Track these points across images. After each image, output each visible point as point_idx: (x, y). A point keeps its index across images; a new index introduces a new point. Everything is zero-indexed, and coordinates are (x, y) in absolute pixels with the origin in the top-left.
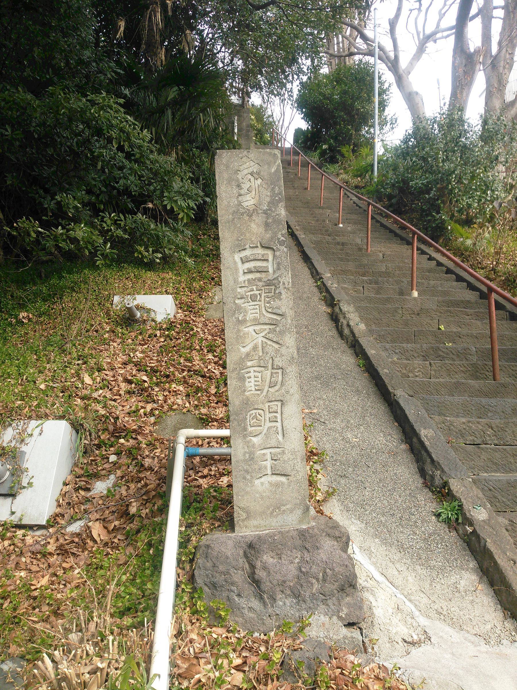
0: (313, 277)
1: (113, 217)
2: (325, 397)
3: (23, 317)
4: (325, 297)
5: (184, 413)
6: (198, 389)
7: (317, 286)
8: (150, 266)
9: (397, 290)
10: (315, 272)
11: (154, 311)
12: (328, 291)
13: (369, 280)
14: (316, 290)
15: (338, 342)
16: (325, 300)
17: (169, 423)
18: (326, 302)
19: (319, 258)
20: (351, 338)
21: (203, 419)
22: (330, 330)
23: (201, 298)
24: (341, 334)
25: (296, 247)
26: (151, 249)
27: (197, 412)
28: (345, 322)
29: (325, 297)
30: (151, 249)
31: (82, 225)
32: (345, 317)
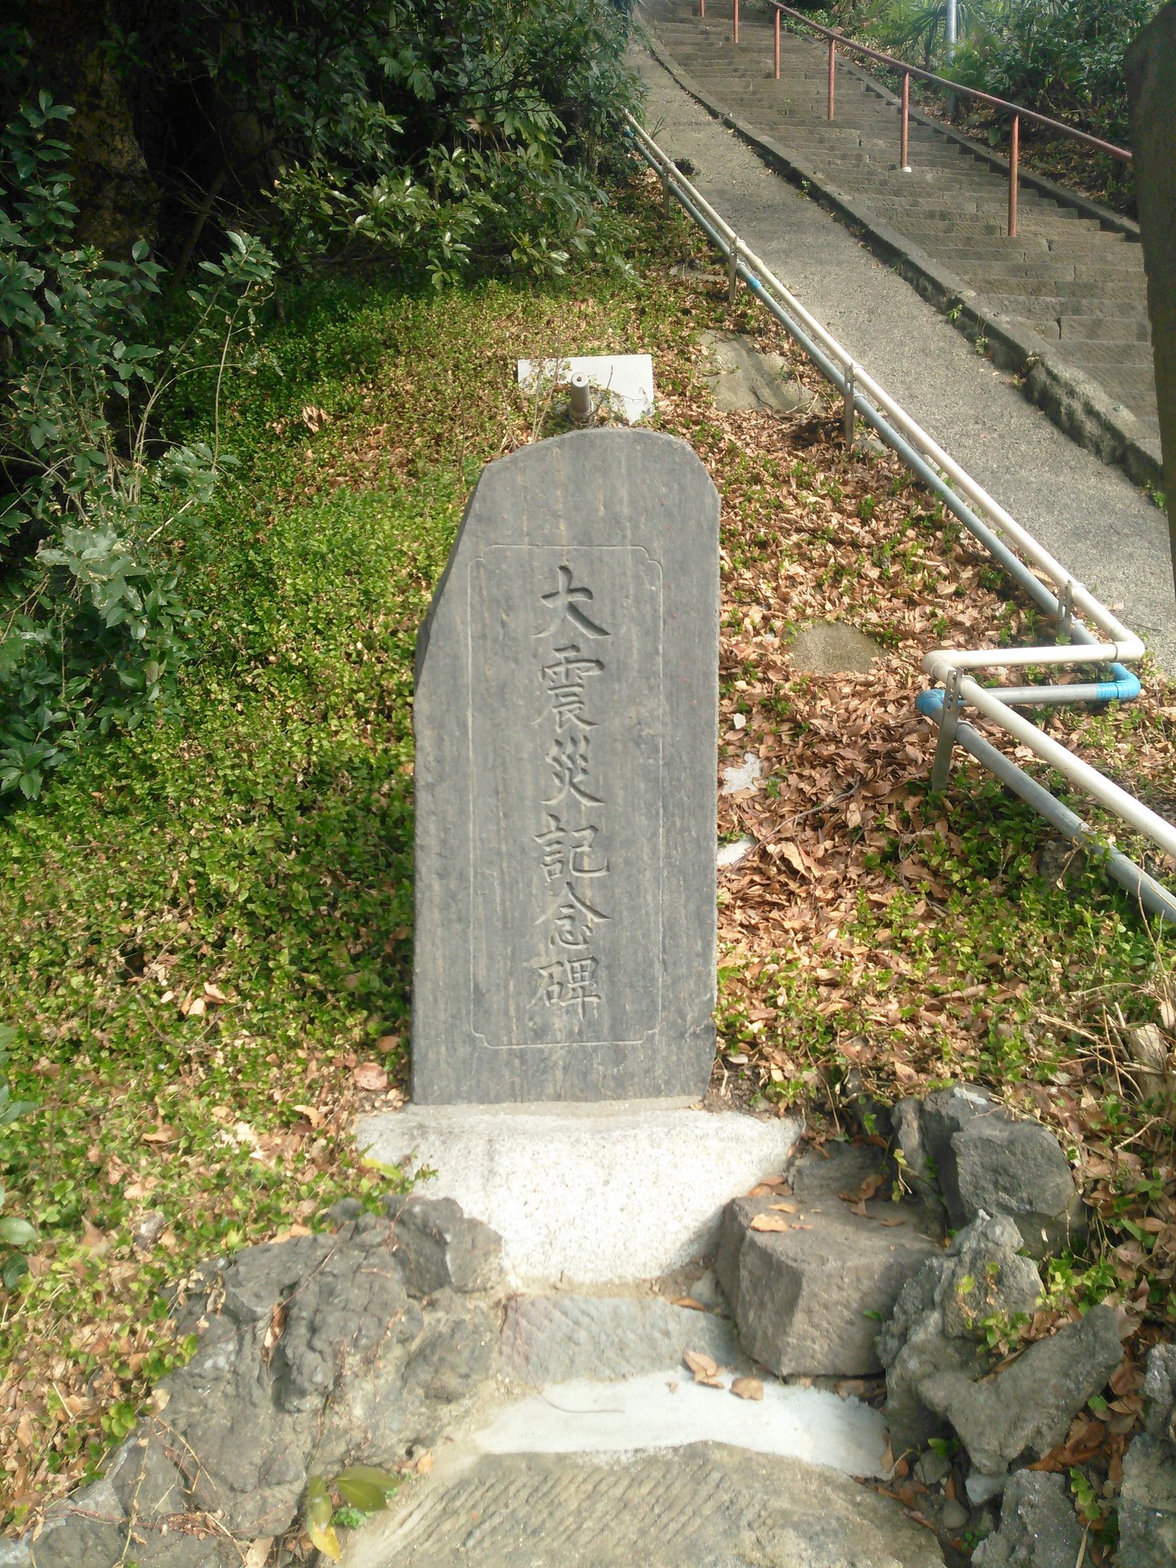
0: (926, 299)
1: (459, 157)
2: (1120, 575)
3: (311, 418)
4: (986, 347)
5: (829, 623)
6: (840, 571)
7: (953, 322)
8: (547, 283)
9: (1134, 327)
10: (930, 287)
11: (617, 396)
12: (991, 331)
13: (1061, 304)
14: (949, 331)
15: (1071, 452)
16: (989, 353)
17: (811, 646)
18: (992, 360)
19: (921, 252)
20: (1108, 443)
21: (879, 634)
22: (1037, 426)
23: (688, 360)
24: (1074, 433)
25: (838, 227)
26: (544, 241)
27: (857, 620)
28: (1077, 406)
29: (986, 347)
30: (544, 241)
31: (408, 183)
32: (1072, 393)
